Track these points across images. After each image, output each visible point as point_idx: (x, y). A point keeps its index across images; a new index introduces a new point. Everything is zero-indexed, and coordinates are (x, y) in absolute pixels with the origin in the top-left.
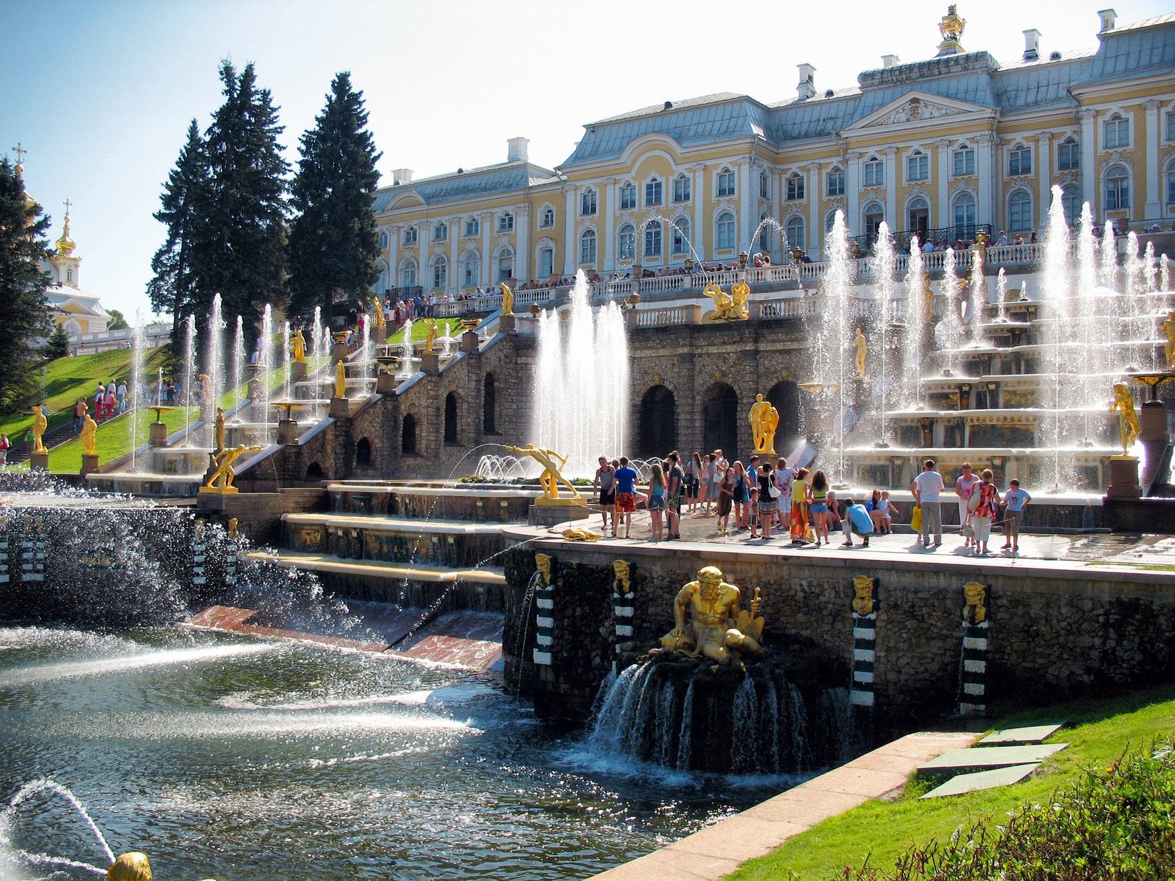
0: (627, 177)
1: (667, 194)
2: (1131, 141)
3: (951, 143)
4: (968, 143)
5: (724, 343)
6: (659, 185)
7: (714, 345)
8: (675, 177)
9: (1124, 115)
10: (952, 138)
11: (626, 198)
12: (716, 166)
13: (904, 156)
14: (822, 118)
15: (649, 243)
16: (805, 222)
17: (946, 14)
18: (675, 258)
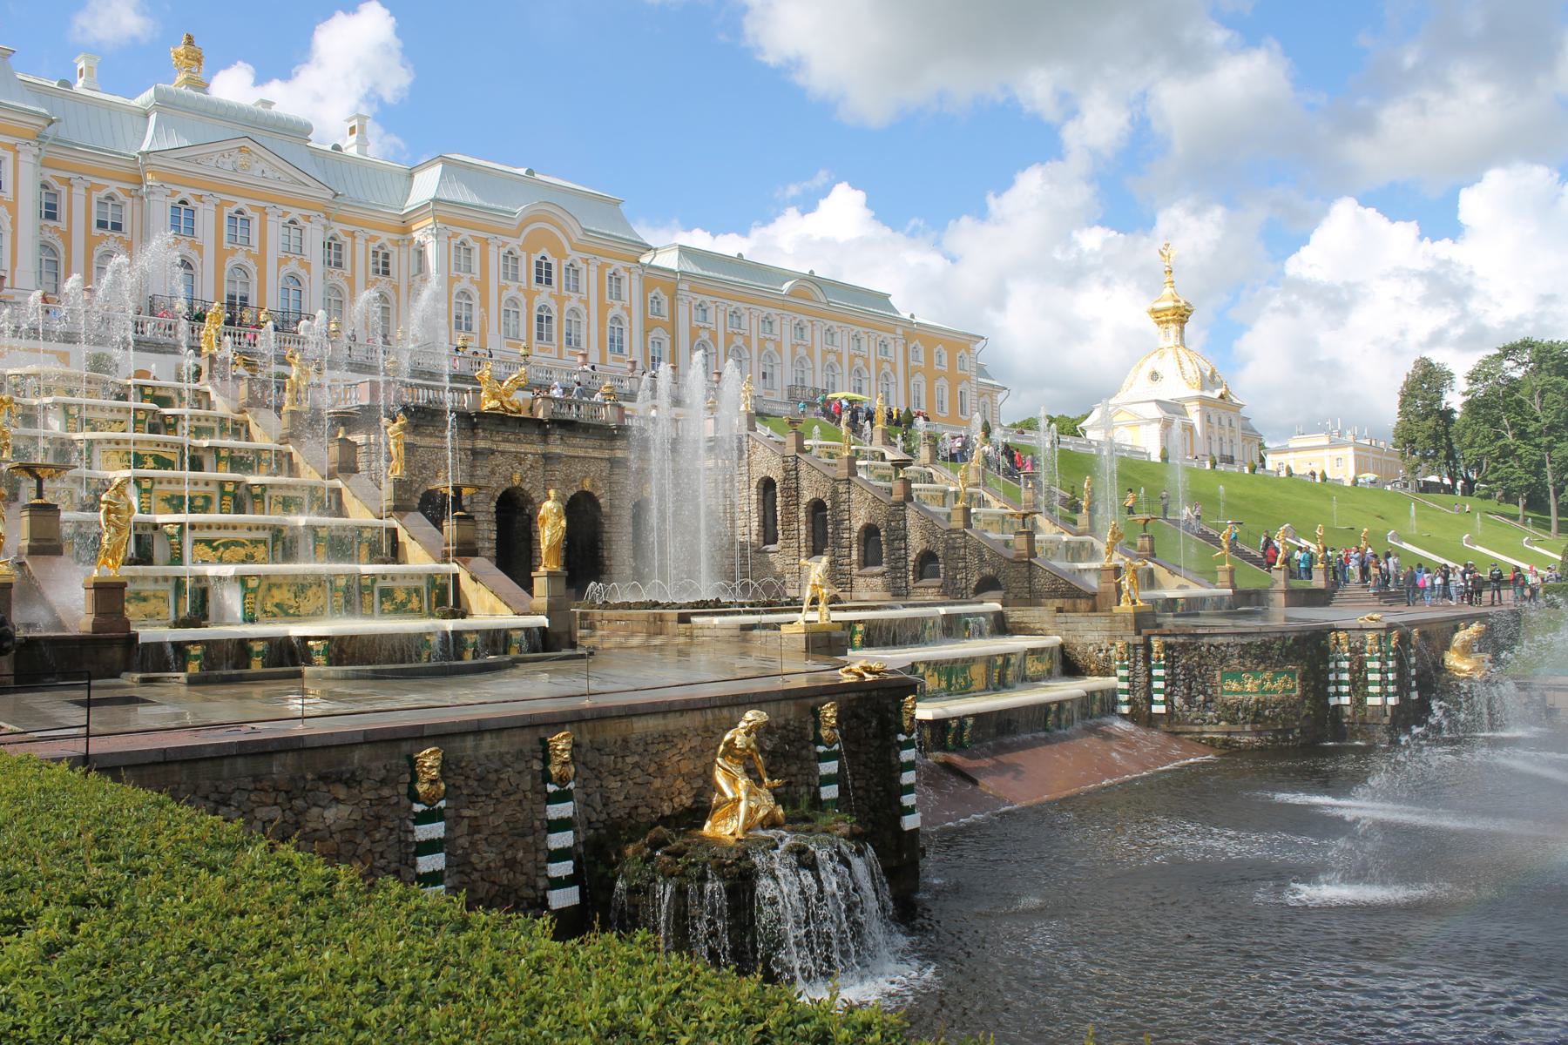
4: (301, 222)
5: (519, 441)
7: (508, 441)
9: (471, 243)
16: (62, 255)
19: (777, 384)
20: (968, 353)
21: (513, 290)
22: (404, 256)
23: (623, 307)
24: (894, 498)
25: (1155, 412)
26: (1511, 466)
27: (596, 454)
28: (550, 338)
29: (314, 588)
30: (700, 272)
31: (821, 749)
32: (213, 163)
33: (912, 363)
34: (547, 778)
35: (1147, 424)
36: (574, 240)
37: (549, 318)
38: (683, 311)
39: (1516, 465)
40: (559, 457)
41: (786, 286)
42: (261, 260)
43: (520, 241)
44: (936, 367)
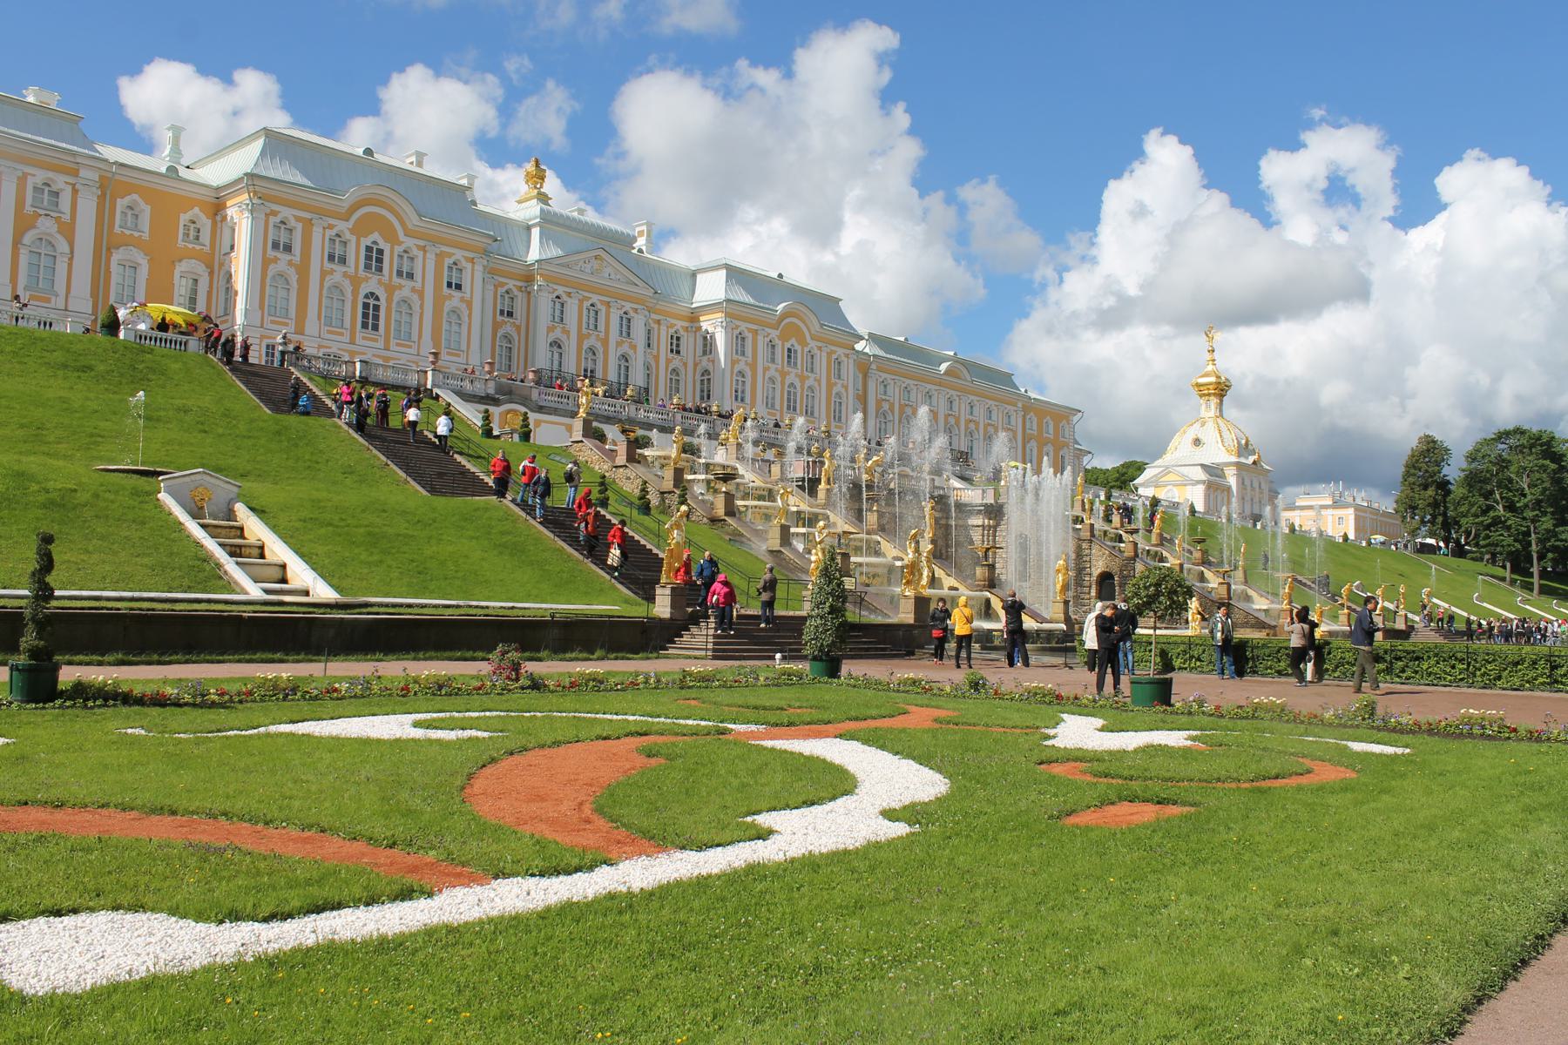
4: (632, 314)
6: (380, 252)
15: (365, 315)
21: (772, 373)
22: (691, 340)
23: (843, 386)
24: (1126, 554)
25: (1200, 475)
26: (1502, 535)
30: (885, 355)
33: (1028, 431)
35: (1193, 485)
38: (871, 386)
39: (1506, 534)
41: (944, 367)
42: (605, 342)
43: (777, 332)
44: (1045, 435)
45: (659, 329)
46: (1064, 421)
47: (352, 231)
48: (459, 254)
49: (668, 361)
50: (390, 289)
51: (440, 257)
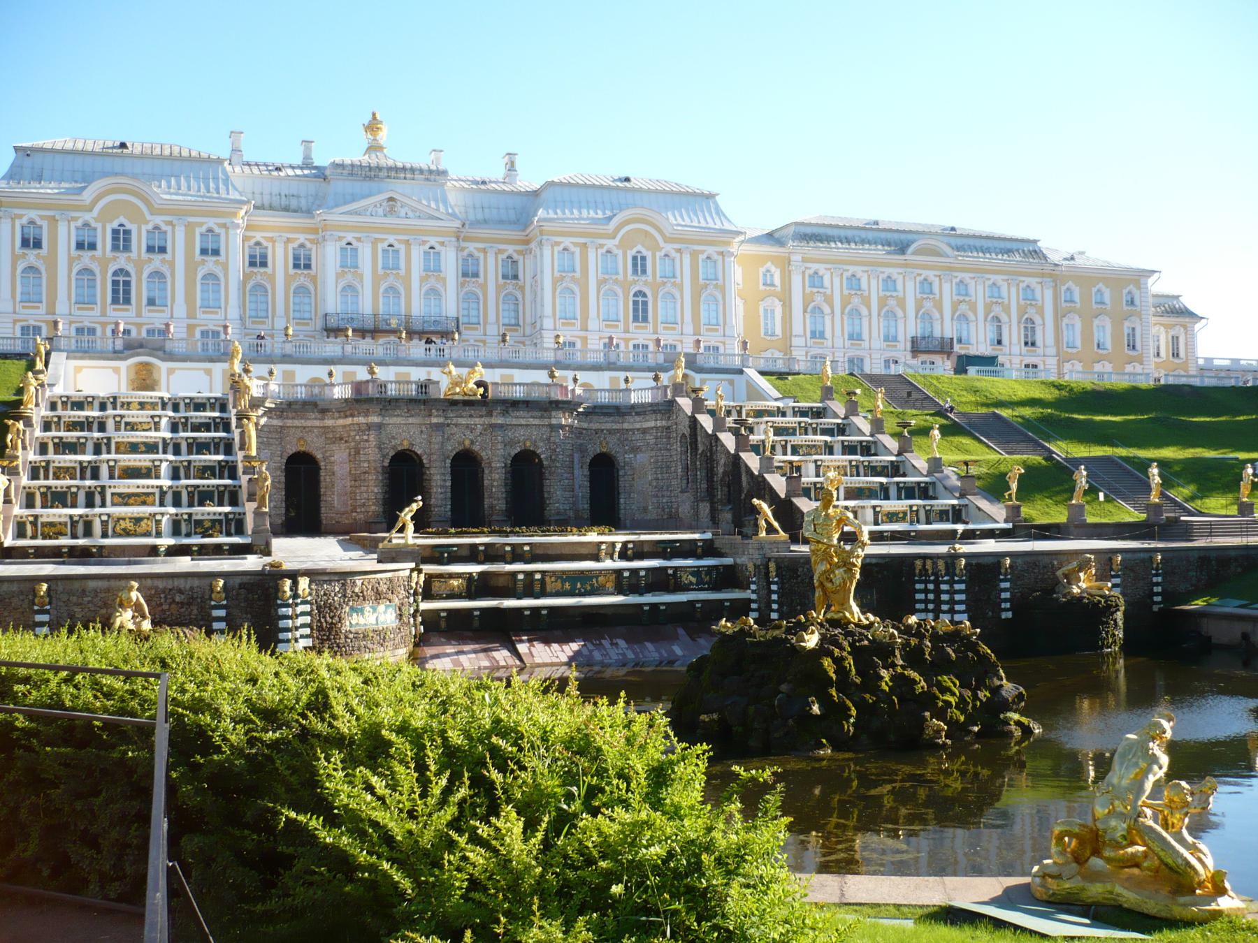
0: (88, 217)
1: (139, 241)
2: (578, 268)
3: (424, 242)
4: (438, 247)
5: (471, 416)
6: (127, 232)
7: (462, 417)
8: (150, 227)
9: (572, 248)
10: (425, 238)
11: (81, 238)
12: (201, 224)
13: (381, 246)
14: (283, 194)
15: (115, 292)
16: (270, 291)
17: (370, 117)
18: (149, 311)
19: (901, 337)
20: (1139, 288)
27: (537, 422)
28: (645, 319)
29: (145, 521)
31: (213, 603)
32: (368, 213)
34: (34, 604)
36: (668, 235)
37: (645, 303)
40: (501, 426)
43: (616, 241)
45: (485, 258)
46: (1131, 286)
47: (96, 220)
48: (211, 222)
49: (499, 289)
50: (140, 265)
51: (190, 228)
